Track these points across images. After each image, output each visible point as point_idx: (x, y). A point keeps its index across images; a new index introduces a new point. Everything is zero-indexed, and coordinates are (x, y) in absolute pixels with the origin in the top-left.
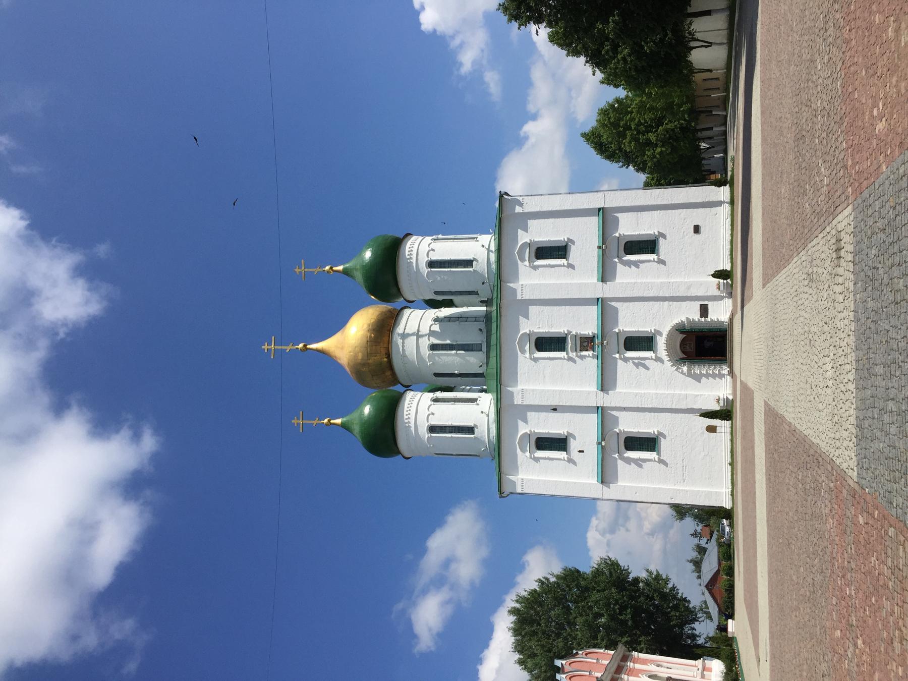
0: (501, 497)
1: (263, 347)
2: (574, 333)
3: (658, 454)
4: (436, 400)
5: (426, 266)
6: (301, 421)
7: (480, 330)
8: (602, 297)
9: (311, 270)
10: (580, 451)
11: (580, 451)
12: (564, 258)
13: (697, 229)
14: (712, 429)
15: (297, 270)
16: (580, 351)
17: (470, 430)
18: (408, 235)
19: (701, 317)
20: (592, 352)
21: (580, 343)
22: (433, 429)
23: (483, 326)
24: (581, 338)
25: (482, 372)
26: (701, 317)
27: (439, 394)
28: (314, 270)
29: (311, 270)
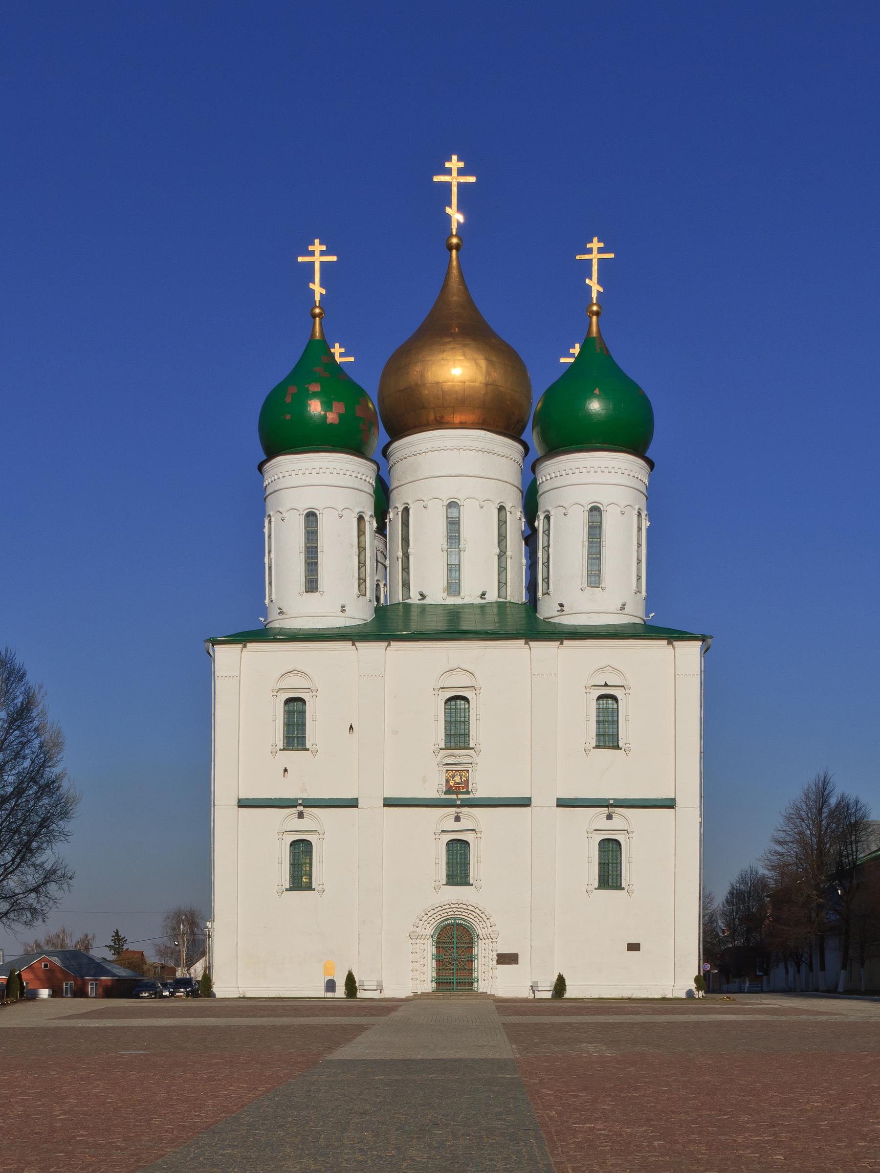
3: (287, 890)
4: (361, 519)
6: (317, 260)
10: (286, 770)
13: (634, 947)
17: (312, 585)
18: (651, 464)
19: (498, 955)
20: (444, 791)
26: (498, 955)
27: (371, 525)
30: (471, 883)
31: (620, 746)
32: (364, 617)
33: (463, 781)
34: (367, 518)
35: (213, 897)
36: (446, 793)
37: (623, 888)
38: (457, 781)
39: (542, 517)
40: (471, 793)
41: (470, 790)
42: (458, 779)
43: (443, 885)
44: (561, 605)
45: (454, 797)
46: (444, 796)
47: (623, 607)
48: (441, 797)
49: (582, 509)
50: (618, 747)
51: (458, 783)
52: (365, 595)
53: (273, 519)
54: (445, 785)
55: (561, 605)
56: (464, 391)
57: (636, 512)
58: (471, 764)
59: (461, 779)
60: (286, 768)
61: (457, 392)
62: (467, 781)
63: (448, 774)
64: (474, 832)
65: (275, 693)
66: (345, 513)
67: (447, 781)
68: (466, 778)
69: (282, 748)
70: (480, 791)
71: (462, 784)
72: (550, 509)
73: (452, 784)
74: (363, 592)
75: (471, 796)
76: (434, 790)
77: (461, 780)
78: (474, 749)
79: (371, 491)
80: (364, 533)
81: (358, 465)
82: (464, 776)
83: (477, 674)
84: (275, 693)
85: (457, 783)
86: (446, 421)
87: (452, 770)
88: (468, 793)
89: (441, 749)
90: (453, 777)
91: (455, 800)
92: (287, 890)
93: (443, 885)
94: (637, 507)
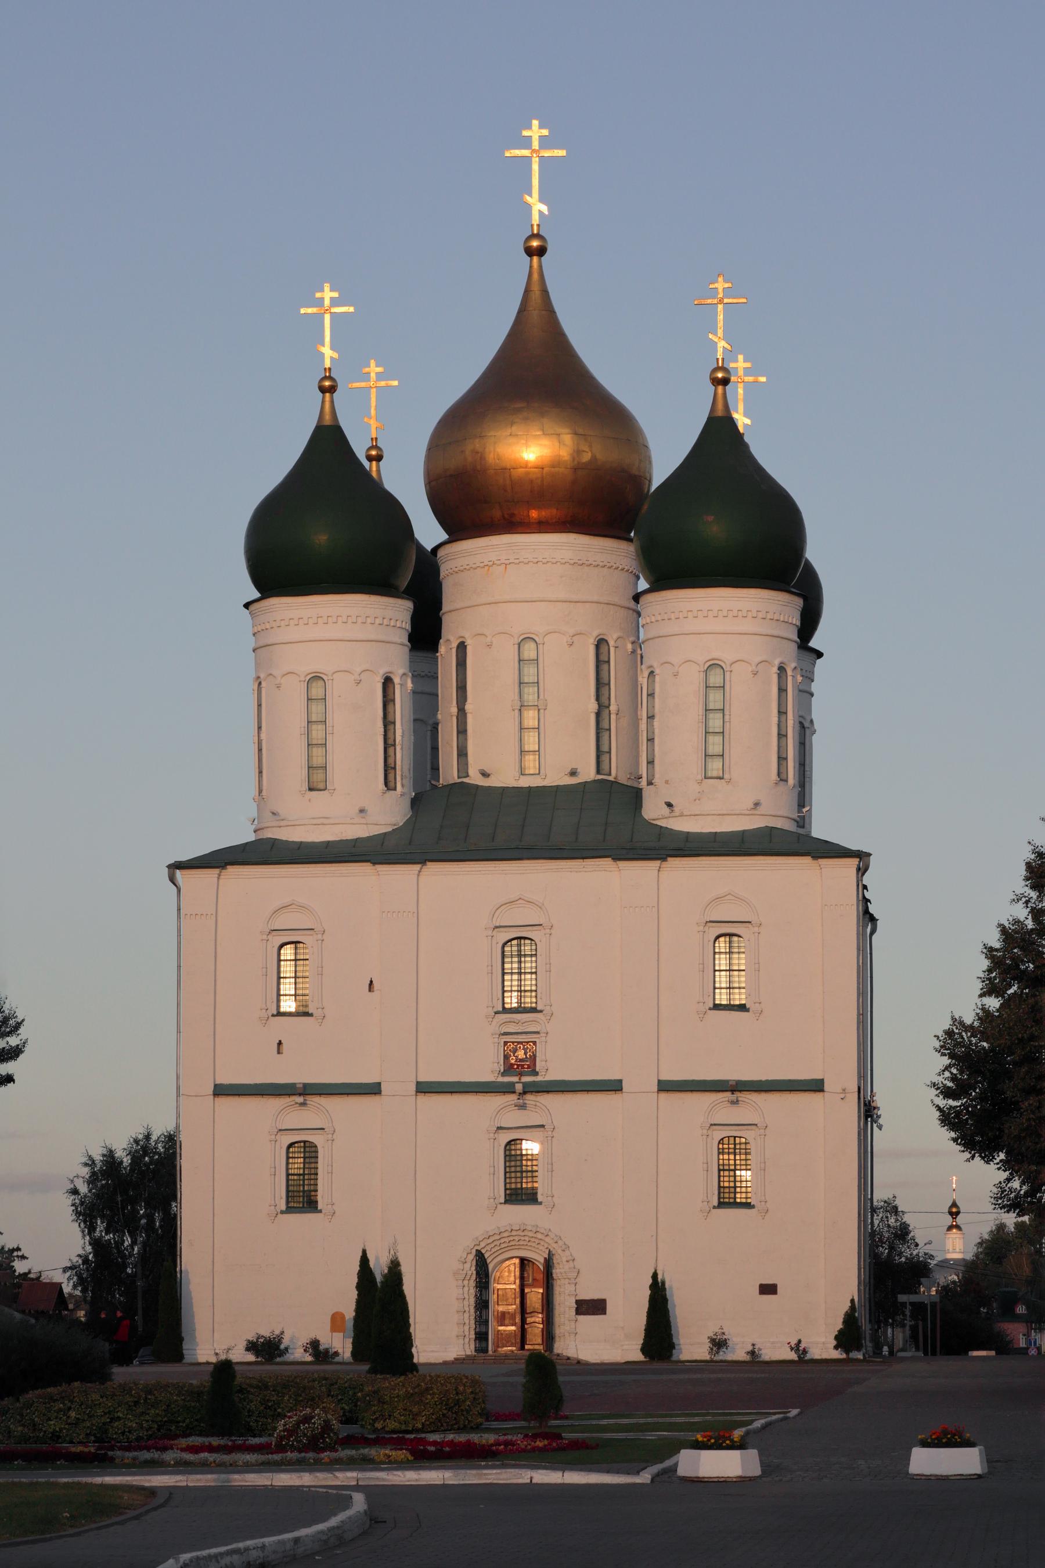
0: (169, 867)
1: (535, 123)
3: (282, 1212)
4: (387, 682)
7: (573, 773)
9: (720, 324)
11: (280, 1043)
13: (768, 1289)
14: (336, 1322)
15: (721, 285)
16: (506, 1043)
19: (577, 1302)
20: (502, 1071)
21: (521, 1043)
23: (588, 773)
24: (535, 1043)
25: (471, 772)
27: (404, 688)
28: (720, 333)
29: (720, 324)
30: (539, 1201)
32: (393, 820)
34: (397, 680)
35: (179, 1223)
36: (503, 1074)
37: (754, 1205)
38: (520, 1057)
41: (537, 1070)
42: (521, 1054)
43: (501, 1203)
44: (669, 805)
45: (515, 1079)
46: (501, 1079)
47: (757, 804)
48: (498, 1080)
51: (521, 1060)
52: (395, 789)
53: (263, 684)
54: (502, 1064)
55: (669, 805)
56: (542, 481)
57: (775, 669)
58: (538, 1033)
59: (525, 1053)
60: (280, 1041)
61: (531, 481)
62: (534, 1058)
63: (508, 1048)
64: (542, 1129)
65: (265, 937)
66: (363, 676)
67: (505, 1056)
68: (533, 1052)
69: (275, 1013)
71: (527, 1061)
72: (655, 665)
73: (513, 1062)
74: (391, 784)
76: (488, 1070)
77: (526, 1056)
78: (541, 1011)
79: (406, 641)
80: (393, 701)
81: (384, 607)
82: (530, 1050)
84: (265, 937)
85: (520, 1059)
86: (519, 520)
87: (513, 1042)
88: (536, 1074)
90: (515, 1051)
91: (513, 1084)
92: (282, 1212)
93: (501, 1203)
94: (777, 662)
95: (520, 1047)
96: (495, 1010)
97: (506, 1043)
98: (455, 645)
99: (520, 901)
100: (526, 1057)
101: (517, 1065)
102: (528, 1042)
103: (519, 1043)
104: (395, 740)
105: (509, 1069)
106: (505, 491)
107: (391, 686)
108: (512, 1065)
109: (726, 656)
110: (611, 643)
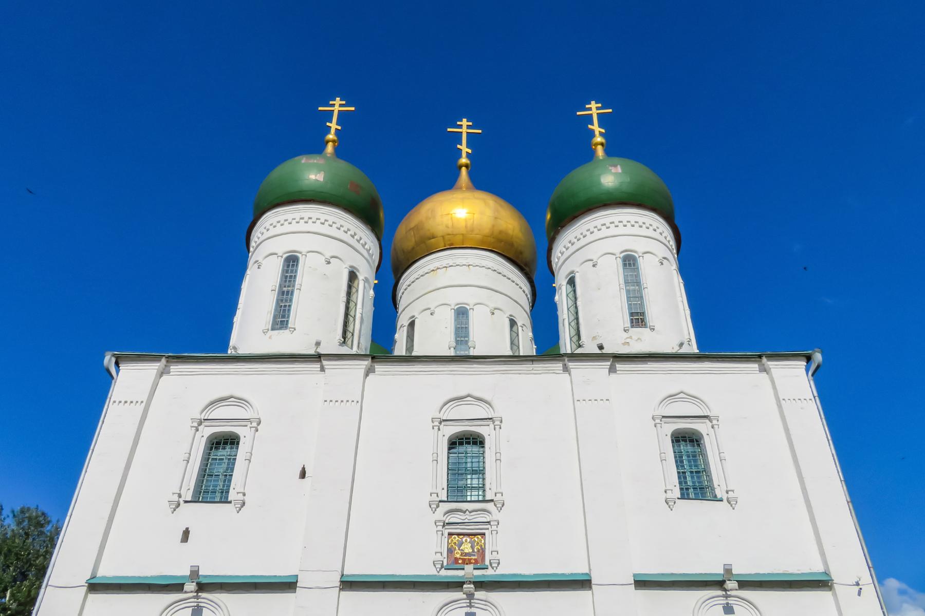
2: (495, 518)
4: (353, 276)
5: (626, 251)
8: (593, 582)
12: (682, 494)
16: (450, 534)
20: (445, 564)
22: (291, 261)
31: (719, 496)
33: (476, 550)
34: (361, 277)
38: (466, 551)
39: (564, 282)
40: (490, 567)
42: (467, 548)
46: (444, 573)
49: (614, 257)
50: (715, 499)
51: (466, 554)
54: (445, 554)
59: (472, 547)
62: (482, 552)
67: (450, 551)
68: (481, 546)
70: (507, 568)
71: (475, 555)
73: (458, 556)
75: (490, 572)
78: (492, 501)
82: (478, 543)
83: (494, 403)
87: (459, 534)
89: (441, 501)
95: (466, 541)
96: (439, 499)
97: (450, 534)
98: (406, 323)
99: (469, 398)
100: (473, 551)
101: (462, 559)
102: (475, 535)
103: (464, 535)
104: (354, 330)
105: (455, 563)
106: (448, 227)
107: (355, 284)
108: (456, 560)
109: (638, 246)
110: (519, 324)
